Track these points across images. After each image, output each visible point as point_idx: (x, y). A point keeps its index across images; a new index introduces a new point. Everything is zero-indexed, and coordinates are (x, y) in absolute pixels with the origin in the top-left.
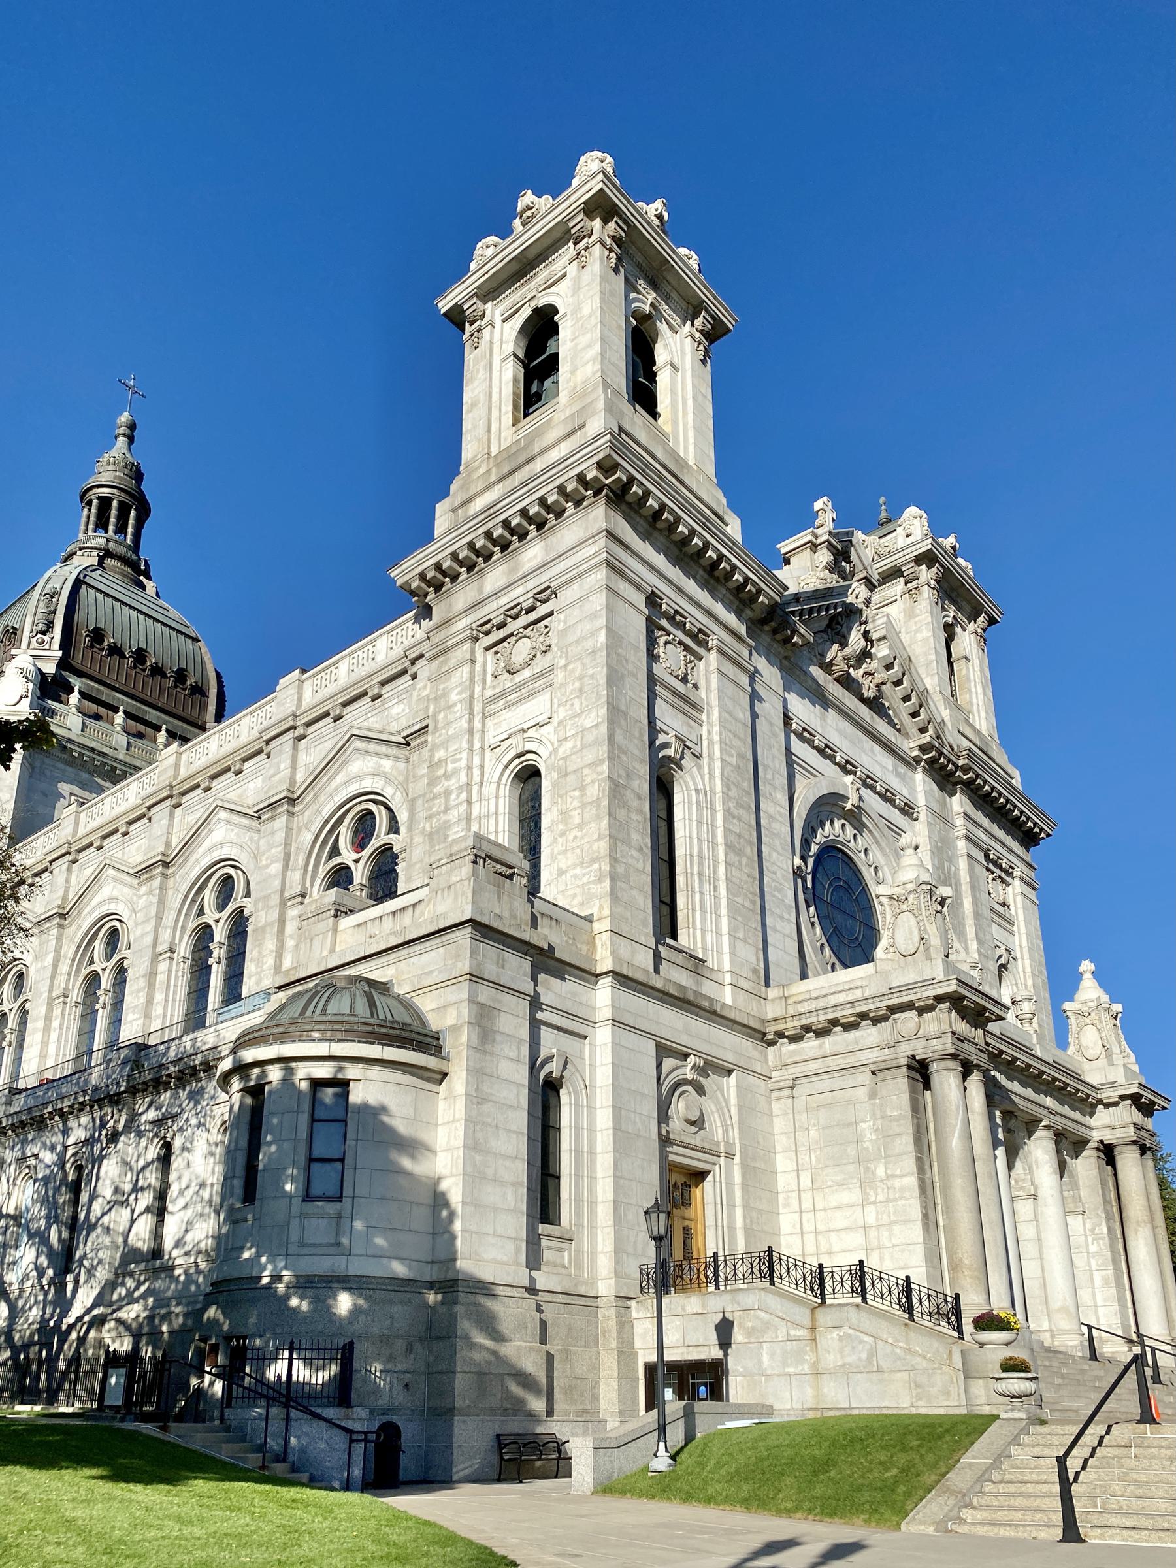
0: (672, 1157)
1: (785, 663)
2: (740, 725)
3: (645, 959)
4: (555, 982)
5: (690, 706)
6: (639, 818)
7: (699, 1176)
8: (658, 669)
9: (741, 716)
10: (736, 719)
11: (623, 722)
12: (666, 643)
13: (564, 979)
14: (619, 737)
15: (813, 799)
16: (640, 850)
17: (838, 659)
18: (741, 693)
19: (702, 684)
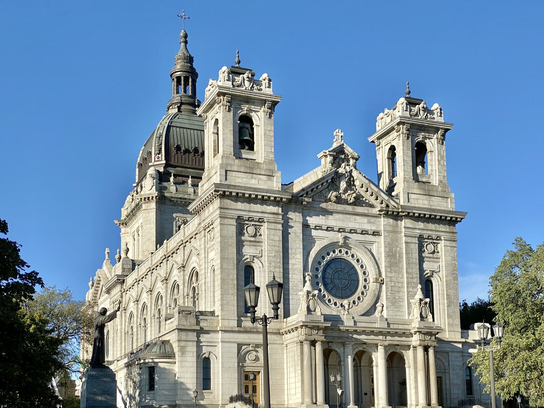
0: (246, 370)
1: (306, 208)
2: (277, 242)
3: (235, 323)
4: (206, 336)
5: (257, 243)
6: (232, 286)
7: (259, 372)
8: (243, 238)
9: (278, 239)
10: (275, 241)
11: (226, 261)
12: (247, 227)
13: (210, 334)
14: (225, 266)
15: (319, 249)
16: (233, 294)
17: (332, 196)
18: (278, 231)
19: (262, 234)
